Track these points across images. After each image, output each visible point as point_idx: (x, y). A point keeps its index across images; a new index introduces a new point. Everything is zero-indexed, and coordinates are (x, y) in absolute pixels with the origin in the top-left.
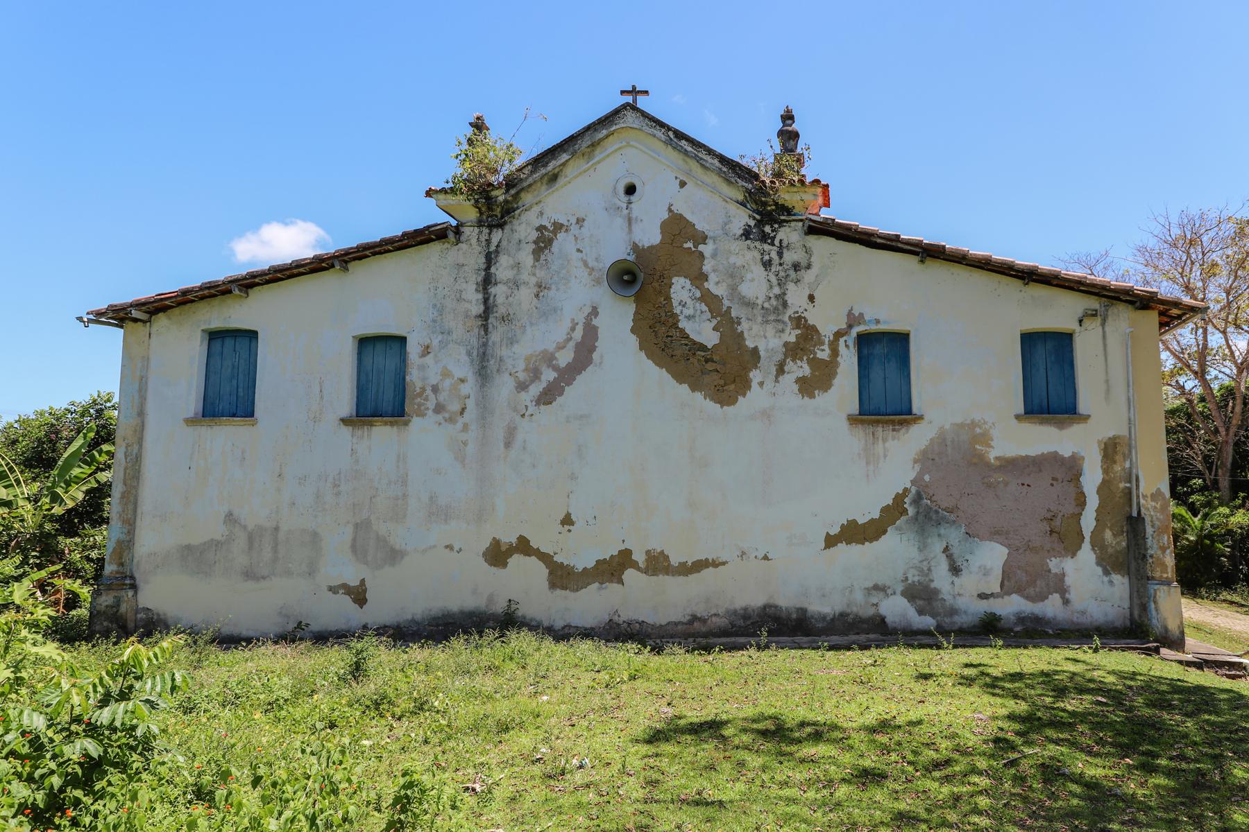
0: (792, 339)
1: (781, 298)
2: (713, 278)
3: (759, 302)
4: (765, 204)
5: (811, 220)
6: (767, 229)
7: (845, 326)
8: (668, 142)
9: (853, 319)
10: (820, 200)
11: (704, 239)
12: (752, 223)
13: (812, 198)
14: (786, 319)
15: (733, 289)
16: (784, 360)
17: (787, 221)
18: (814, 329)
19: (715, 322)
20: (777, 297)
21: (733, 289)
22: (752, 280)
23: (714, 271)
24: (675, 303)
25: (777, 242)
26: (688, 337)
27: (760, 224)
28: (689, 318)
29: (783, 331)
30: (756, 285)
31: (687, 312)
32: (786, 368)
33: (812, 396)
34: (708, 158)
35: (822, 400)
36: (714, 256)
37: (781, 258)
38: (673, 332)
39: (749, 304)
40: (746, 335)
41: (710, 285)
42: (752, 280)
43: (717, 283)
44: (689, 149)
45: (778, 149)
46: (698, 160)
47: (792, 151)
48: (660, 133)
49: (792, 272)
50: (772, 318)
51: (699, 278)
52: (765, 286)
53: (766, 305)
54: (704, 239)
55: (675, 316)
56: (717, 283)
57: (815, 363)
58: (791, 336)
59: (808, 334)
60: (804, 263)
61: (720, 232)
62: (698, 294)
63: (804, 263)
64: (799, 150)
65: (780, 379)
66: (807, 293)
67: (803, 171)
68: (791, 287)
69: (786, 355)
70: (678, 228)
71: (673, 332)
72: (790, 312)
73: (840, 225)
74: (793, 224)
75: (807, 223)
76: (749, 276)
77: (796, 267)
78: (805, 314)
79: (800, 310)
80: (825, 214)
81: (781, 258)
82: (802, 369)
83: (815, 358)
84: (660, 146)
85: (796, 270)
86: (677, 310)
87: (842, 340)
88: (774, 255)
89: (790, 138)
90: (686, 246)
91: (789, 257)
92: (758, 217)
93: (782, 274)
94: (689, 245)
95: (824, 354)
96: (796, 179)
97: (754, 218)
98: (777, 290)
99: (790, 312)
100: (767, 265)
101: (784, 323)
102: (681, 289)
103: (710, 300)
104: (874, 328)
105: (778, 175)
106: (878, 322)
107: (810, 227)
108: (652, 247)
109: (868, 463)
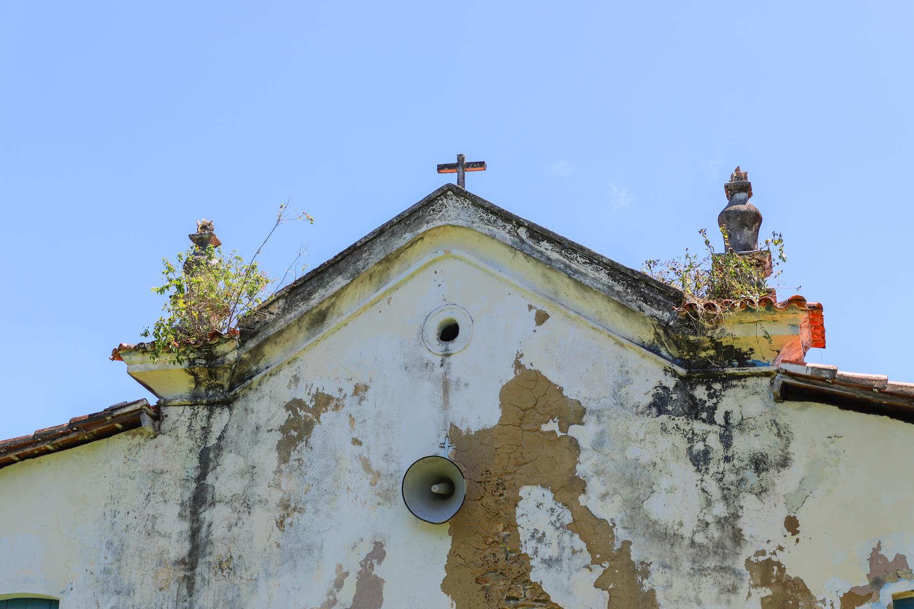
1: (730, 523)
2: (595, 486)
3: (686, 531)
4: (695, 347)
5: (787, 373)
6: (700, 392)
7: (865, 582)
8: (518, 247)
10: (805, 335)
11: (578, 414)
12: (671, 382)
13: (786, 331)
14: (740, 565)
15: (635, 507)
17: (739, 377)
18: (798, 586)
19: (598, 571)
20: (721, 522)
21: (635, 507)
22: (671, 490)
23: (598, 473)
24: (524, 535)
25: (719, 417)
26: (547, 600)
27: (685, 383)
28: (549, 563)
29: (734, 590)
30: (680, 499)
31: (547, 551)
34: (589, 270)
36: (598, 445)
38: (519, 590)
39: (665, 537)
40: (660, 596)
41: (590, 501)
42: (671, 490)
43: (604, 497)
44: (555, 256)
45: (719, 245)
46: (570, 274)
47: (747, 247)
48: (503, 232)
49: (750, 475)
50: (711, 563)
51: (570, 487)
52: (697, 500)
53: (700, 538)
54: (578, 414)
55: (523, 559)
56: (604, 497)
60: (774, 456)
61: (610, 401)
62: (567, 518)
63: (774, 456)
64: (761, 245)
66: (782, 514)
67: (770, 283)
68: (749, 502)
70: (532, 398)
71: (519, 590)
72: (747, 552)
73: (848, 382)
74: (751, 382)
75: (780, 379)
76: (664, 482)
77: (759, 463)
78: (780, 557)
79: (770, 548)
80: (815, 359)
84: (503, 255)
85: (758, 470)
86: (528, 548)
88: (714, 441)
89: (743, 225)
90: (545, 428)
91: (743, 445)
92: (682, 371)
93: (730, 477)
94: (552, 426)
96: (756, 298)
97: (675, 374)
98: (720, 509)
99: (747, 552)
100: (700, 460)
101: (735, 573)
102: (535, 510)
103: (587, 526)
105: (721, 293)
107: (785, 388)
108: (484, 432)
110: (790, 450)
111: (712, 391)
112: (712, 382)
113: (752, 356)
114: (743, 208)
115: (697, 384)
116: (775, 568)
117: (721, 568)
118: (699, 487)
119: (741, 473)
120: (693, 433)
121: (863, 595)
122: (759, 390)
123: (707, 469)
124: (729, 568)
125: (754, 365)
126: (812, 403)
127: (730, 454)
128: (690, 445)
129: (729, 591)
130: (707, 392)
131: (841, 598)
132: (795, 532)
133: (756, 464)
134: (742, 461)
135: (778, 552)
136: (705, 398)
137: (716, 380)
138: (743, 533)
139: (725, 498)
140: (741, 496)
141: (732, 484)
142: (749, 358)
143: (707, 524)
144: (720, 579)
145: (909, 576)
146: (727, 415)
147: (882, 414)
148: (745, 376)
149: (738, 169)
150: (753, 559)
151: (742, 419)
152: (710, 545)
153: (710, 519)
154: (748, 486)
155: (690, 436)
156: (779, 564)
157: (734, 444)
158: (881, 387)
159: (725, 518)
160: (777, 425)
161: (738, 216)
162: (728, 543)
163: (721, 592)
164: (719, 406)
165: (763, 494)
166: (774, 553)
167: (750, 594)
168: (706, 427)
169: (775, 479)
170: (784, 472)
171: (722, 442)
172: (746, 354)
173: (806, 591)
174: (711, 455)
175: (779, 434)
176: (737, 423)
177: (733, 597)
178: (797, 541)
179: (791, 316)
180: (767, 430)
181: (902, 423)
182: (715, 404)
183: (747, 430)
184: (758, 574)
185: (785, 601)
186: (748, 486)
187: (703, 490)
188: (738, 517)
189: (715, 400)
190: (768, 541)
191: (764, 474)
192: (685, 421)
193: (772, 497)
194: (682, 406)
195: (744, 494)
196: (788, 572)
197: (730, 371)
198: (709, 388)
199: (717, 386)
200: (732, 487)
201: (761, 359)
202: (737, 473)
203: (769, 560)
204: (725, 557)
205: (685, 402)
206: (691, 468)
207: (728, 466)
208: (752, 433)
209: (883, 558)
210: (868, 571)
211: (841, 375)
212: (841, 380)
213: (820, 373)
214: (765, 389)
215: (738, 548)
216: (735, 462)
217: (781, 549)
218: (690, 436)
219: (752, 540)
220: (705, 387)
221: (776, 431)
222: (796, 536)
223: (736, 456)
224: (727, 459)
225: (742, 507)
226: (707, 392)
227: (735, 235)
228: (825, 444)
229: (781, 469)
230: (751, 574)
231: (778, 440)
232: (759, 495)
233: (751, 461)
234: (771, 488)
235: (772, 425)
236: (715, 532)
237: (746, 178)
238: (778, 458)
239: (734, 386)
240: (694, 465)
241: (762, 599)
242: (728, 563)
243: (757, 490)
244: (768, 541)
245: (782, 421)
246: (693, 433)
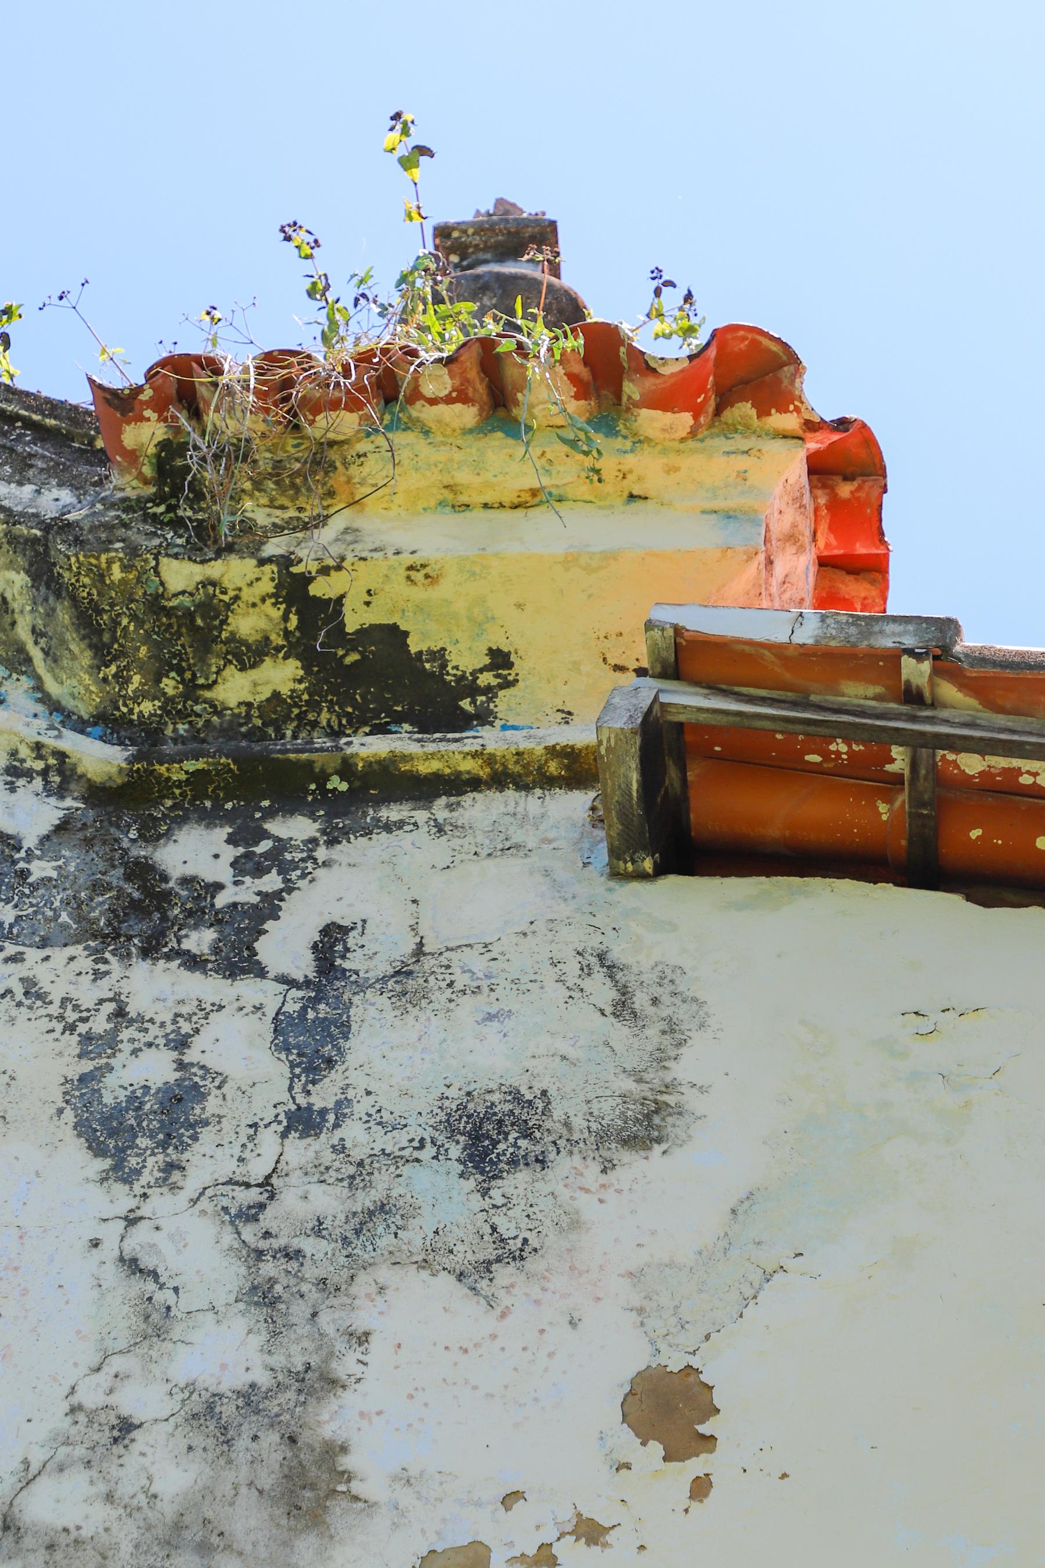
6: (196, 853)
17: (424, 789)
25: (286, 946)
68: (409, 1315)
77: (490, 1137)
92: (100, 758)
98: (225, 1352)
100: (136, 1133)
111: (264, 846)
113: (504, 702)
115: (182, 821)
118: (110, 1250)
120: (120, 1013)
123: (171, 1167)
127: (323, 1096)
128: (87, 1066)
130: (230, 853)
136: (222, 872)
137: (291, 802)
139: (263, 1297)
141: (318, 1229)
143: (126, 1427)
151: (419, 951)
152: (126, 1535)
153: (144, 1400)
154: (415, 1237)
155: (100, 1024)
159: (250, 1398)
162: (248, 1521)
164: (290, 905)
165: (504, 1274)
168: (208, 987)
174: (212, 1105)
175: (623, 1008)
186: (415, 1237)
187: (132, 1266)
188: (333, 1383)
189: (272, 882)
190: (511, 1499)
191: (516, 1183)
192: (86, 963)
194: (76, 905)
195: (384, 1274)
198: (245, 835)
199: (297, 828)
200: (309, 1245)
205: (97, 887)
206: (78, 1162)
207: (299, 1151)
208: (468, 1008)
216: (353, 1132)
218: (100, 1024)
219: (405, 1497)
220: (223, 832)
222: (696, 1466)
223: (362, 1107)
225: (363, 1338)
226: (230, 853)
229: (625, 1156)
231: (620, 1032)
232: (475, 1274)
235: (586, 971)
236: (167, 1469)
240: (98, 1150)
243: (464, 1256)
244: (511, 1499)
246: (120, 1013)
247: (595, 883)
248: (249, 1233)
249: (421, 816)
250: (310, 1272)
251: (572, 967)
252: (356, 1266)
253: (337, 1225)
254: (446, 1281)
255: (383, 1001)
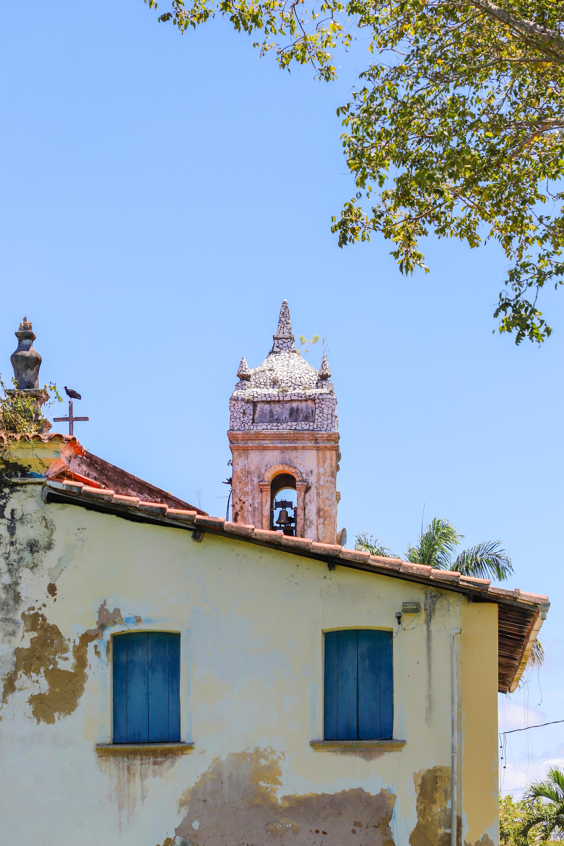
0: (26, 644)
7: (95, 627)
9: (106, 618)
14: (18, 617)
16: (15, 673)
17: (22, 485)
18: (54, 631)
29: (13, 634)
32: (17, 684)
33: (50, 720)
35: (63, 724)
37: (12, 534)
49: (27, 554)
57: (54, 676)
58: (25, 640)
59: (47, 636)
60: (43, 542)
63: (43, 542)
65: (10, 697)
66: (46, 582)
68: (25, 573)
69: (17, 666)
72: (23, 608)
74: (29, 488)
77: (33, 547)
78: (44, 611)
79: (37, 606)
81: (12, 534)
82: (37, 684)
83: (55, 670)
87: (91, 645)
89: (27, 367)
91: (24, 533)
93: (13, 557)
95: (67, 664)
99: (23, 608)
101: (15, 622)
104: (133, 628)
106: (138, 620)
109: (120, 807)
110: (54, 537)
111: (3, 494)
112: (3, 487)
113: (30, 469)
114: (27, 354)
116: (40, 619)
117: (6, 619)
119: (21, 553)
121: (93, 635)
122: (34, 494)
124: (11, 619)
125: (31, 476)
126: (69, 505)
127: (14, 540)
129: (10, 634)
131: (80, 638)
132: (53, 594)
133: (31, 547)
134: (22, 545)
135: (42, 608)
138: (21, 595)
139: (10, 571)
140: (20, 570)
141: (15, 561)
142: (28, 471)
144: (5, 627)
145: (121, 622)
146: (13, 511)
147: (112, 514)
148: (26, 484)
149: (25, 320)
150: (27, 613)
151: (23, 515)
154: (25, 563)
156: (43, 616)
157: (17, 533)
158: (108, 500)
159: (10, 585)
160: (45, 519)
161: (23, 360)
162: (11, 602)
163: (5, 635)
164: (7, 505)
165: (35, 568)
166: (40, 609)
167: (23, 636)
169: (43, 558)
170: (49, 553)
171: (9, 531)
172: (26, 468)
173: (59, 633)
175: (46, 527)
176: (19, 518)
177: (12, 638)
178: (55, 600)
179: (55, 446)
180: (39, 523)
181: (124, 520)
182: (5, 504)
183: (26, 523)
184: (29, 623)
185: (46, 640)
186: (25, 563)
188: (18, 584)
189: (4, 501)
190: (37, 601)
191: (35, 554)
193: (40, 570)
196: (48, 621)
197: (15, 480)
200: (14, 563)
201: (36, 472)
202: (18, 553)
203: (37, 613)
204: (8, 612)
207: (12, 548)
209: (107, 611)
210: (97, 619)
211: (85, 491)
212: (84, 494)
213: (72, 489)
214: (39, 494)
215: (17, 606)
216: (17, 545)
217: (44, 605)
219: (26, 600)
221: (44, 524)
222: (54, 597)
223: (18, 542)
224: (12, 544)
225: (21, 577)
227: (22, 374)
228: (75, 534)
229: (47, 551)
230: (25, 623)
231: (46, 530)
232: (32, 568)
233: (28, 545)
234: (40, 564)
237: (30, 328)
238: (45, 543)
239: (18, 491)
241: (31, 639)
242: (10, 616)
243: (31, 566)
244: (37, 601)
245: (49, 517)
247: (42, 504)
248: (8, 561)
249: (22, 489)
250: (15, 567)
251: (40, 519)
252: (20, 567)
253: (17, 560)
254: (29, 569)
255: (19, 523)
